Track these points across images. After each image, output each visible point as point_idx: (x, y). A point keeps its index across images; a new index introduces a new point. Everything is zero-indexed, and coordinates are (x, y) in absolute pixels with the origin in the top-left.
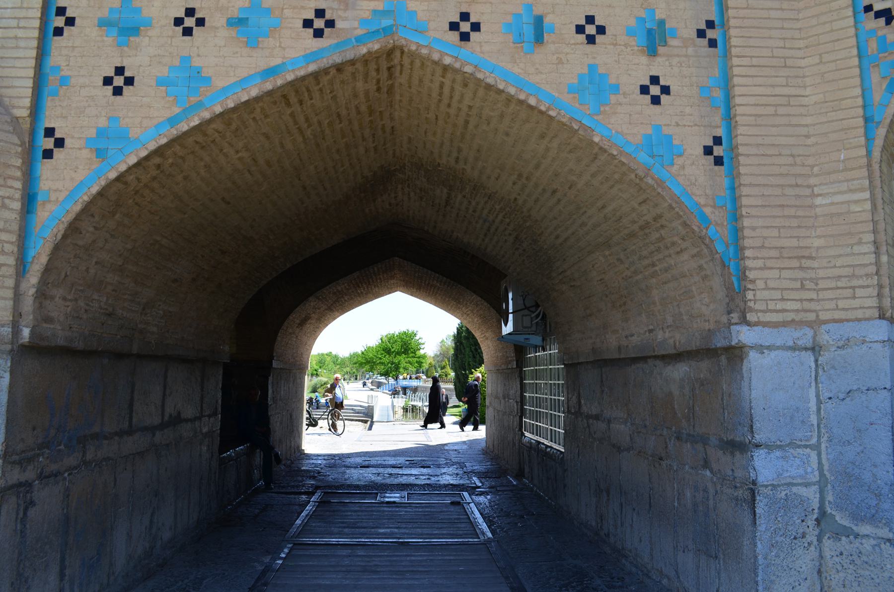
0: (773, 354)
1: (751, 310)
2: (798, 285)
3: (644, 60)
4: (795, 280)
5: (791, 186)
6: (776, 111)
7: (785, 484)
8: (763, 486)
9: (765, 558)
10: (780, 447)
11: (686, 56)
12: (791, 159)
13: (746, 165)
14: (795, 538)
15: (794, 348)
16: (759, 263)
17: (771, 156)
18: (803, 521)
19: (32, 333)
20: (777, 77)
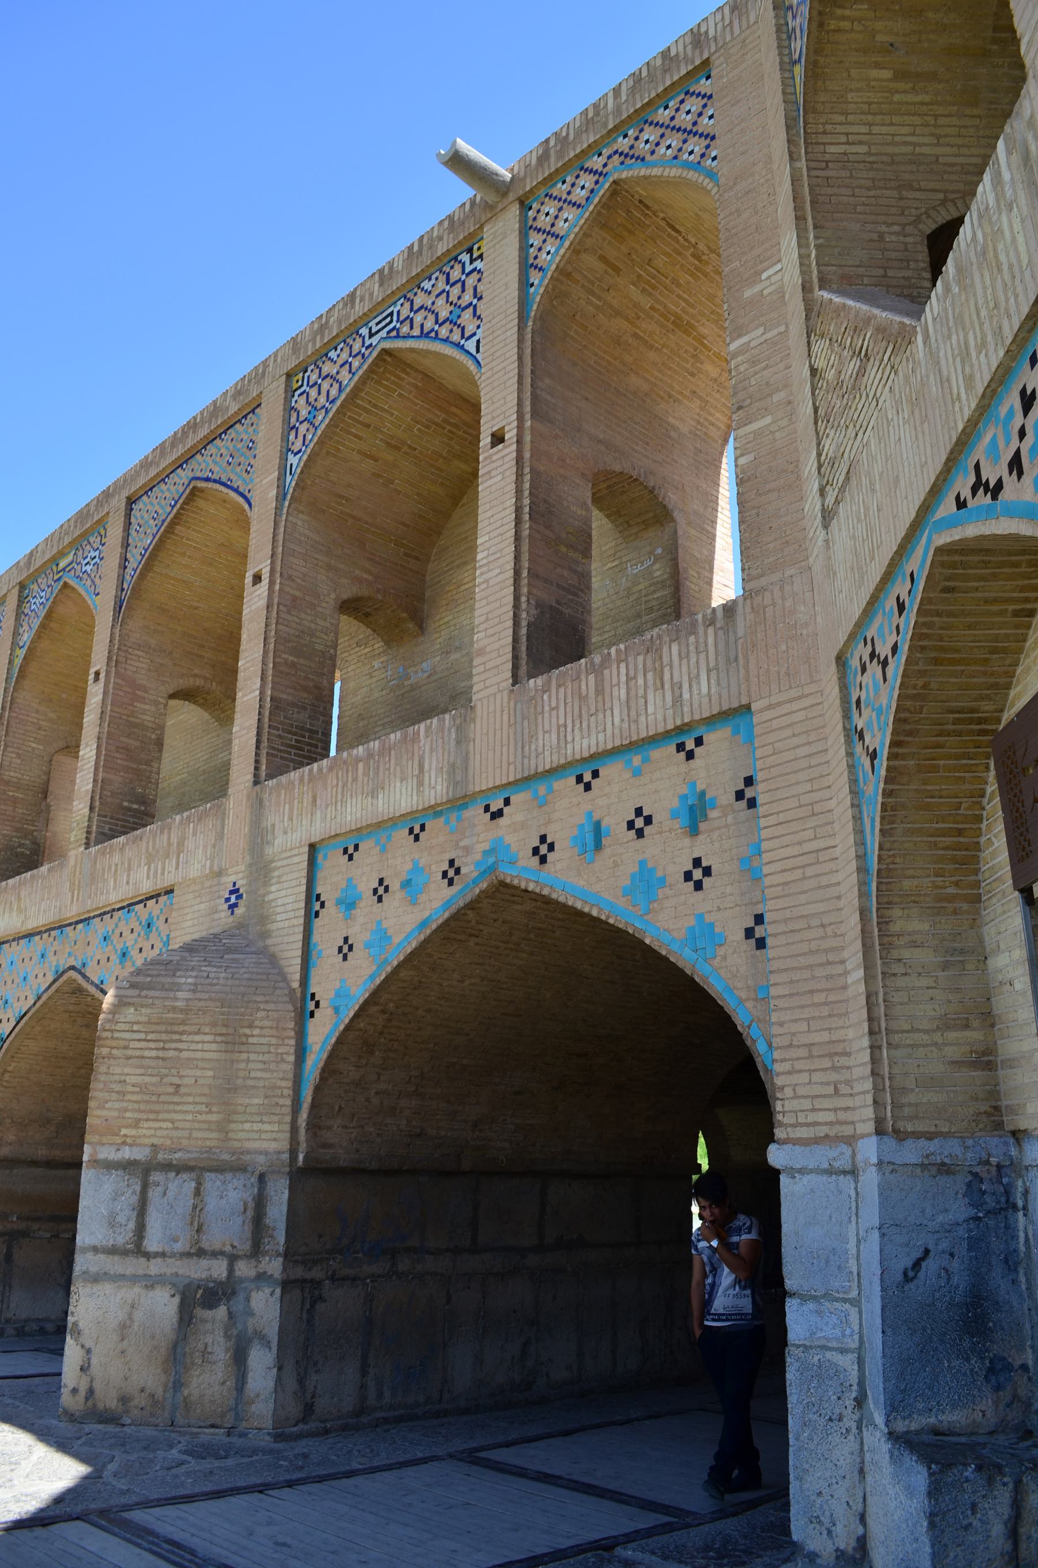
0: (806, 1179)
1: (781, 1124)
2: (831, 1090)
3: (687, 841)
4: (828, 1084)
5: (821, 965)
6: (803, 874)
7: (819, 1347)
8: (793, 1345)
9: (797, 1439)
10: (814, 1298)
12: (821, 930)
13: (773, 948)
14: (830, 1420)
15: (830, 1172)
16: (786, 1066)
17: (799, 931)
18: (839, 1398)
19: (306, 1158)
20: (804, 830)
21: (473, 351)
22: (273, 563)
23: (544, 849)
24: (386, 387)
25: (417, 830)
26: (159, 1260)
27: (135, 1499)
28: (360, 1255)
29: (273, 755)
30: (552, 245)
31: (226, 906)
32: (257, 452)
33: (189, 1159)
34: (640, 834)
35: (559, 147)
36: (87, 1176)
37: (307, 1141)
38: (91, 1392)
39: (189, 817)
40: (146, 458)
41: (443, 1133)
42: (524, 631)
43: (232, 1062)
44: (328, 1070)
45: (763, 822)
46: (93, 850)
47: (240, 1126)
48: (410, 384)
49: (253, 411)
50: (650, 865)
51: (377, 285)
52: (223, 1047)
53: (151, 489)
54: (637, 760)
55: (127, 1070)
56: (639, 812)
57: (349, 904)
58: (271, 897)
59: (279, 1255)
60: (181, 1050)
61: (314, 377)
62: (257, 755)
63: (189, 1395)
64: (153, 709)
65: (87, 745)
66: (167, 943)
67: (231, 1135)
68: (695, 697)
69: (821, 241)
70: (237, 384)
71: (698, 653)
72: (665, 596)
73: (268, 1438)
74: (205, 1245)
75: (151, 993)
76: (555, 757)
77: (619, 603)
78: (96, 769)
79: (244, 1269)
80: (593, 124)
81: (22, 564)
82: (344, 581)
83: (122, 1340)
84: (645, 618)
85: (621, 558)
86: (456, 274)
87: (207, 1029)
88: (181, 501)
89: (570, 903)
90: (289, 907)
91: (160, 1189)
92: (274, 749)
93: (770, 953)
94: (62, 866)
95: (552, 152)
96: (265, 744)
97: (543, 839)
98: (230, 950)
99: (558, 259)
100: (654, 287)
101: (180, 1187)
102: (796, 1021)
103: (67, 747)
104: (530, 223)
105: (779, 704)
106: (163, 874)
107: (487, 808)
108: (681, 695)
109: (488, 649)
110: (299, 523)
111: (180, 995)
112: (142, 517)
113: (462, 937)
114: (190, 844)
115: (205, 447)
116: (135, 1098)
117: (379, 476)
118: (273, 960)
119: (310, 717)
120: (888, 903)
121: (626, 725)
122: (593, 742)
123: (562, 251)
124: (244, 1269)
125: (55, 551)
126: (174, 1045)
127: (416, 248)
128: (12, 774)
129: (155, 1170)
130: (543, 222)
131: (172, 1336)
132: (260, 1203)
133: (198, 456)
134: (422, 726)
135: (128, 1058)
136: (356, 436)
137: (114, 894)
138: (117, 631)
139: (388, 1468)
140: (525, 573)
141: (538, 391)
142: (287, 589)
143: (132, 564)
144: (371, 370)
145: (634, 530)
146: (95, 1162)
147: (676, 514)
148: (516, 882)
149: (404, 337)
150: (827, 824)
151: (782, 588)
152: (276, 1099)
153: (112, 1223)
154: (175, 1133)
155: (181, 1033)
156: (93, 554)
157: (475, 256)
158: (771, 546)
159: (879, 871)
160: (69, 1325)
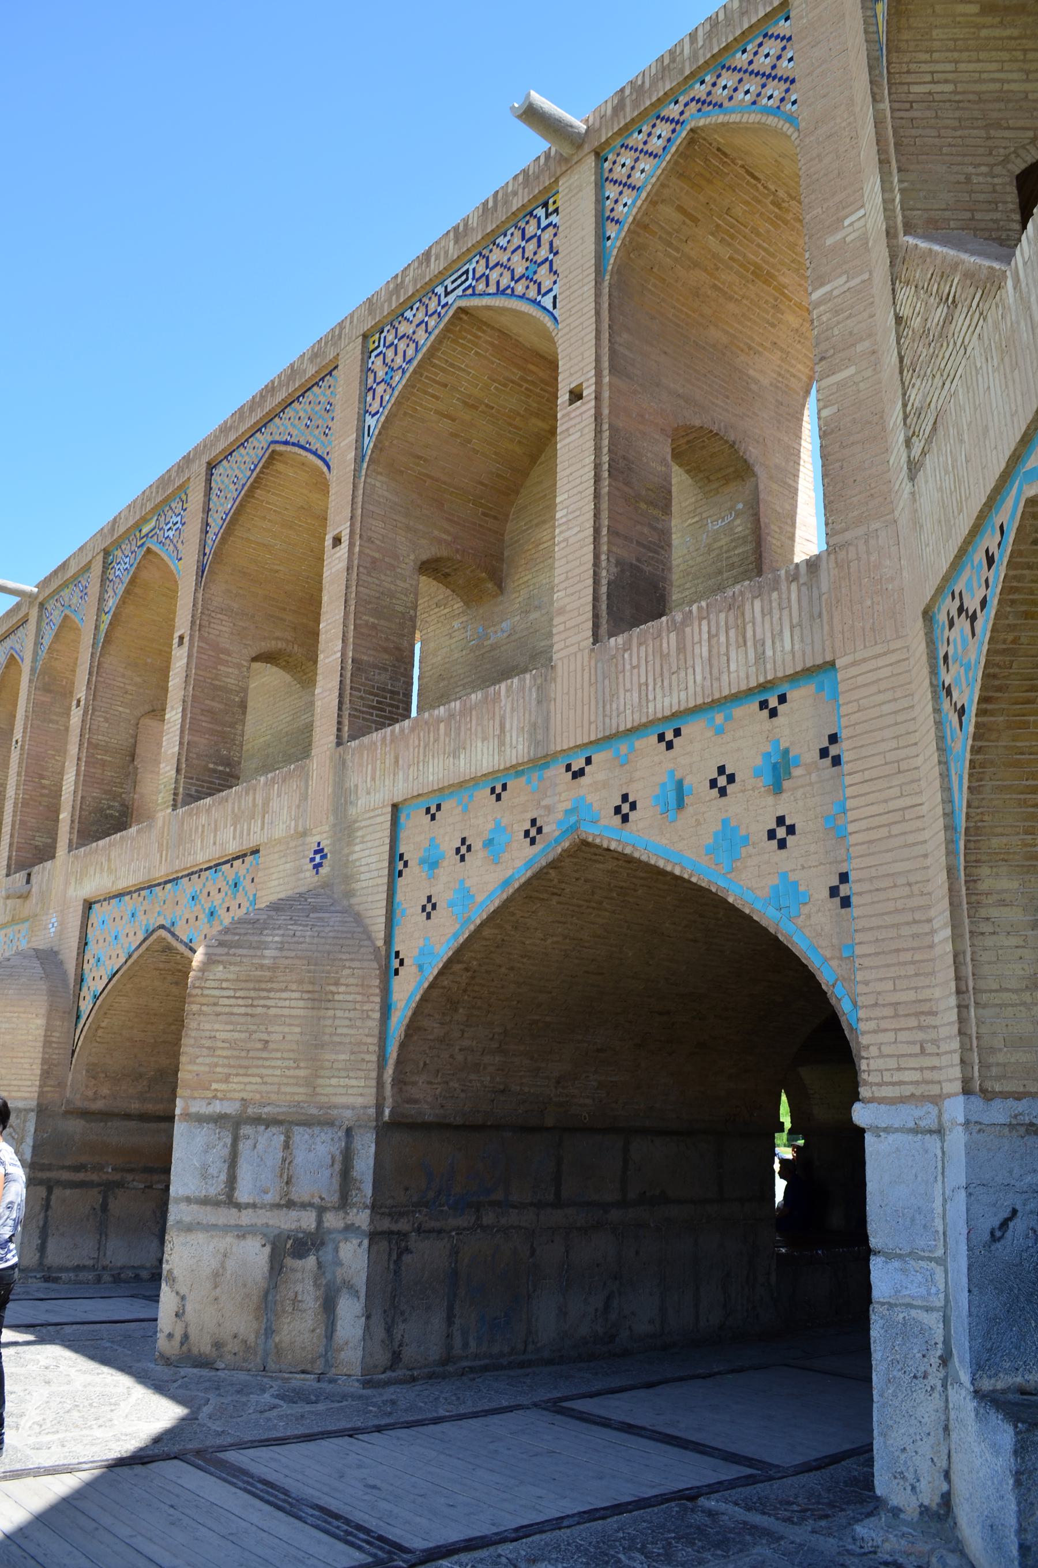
0: (891, 1138)
1: (866, 1083)
2: (917, 1049)
3: (770, 800)
4: (914, 1043)
5: (907, 923)
6: (889, 832)
7: (904, 1305)
8: (878, 1303)
9: (881, 1396)
10: (900, 1257)
11: (811, 784)
12: (907, 888)
13: (859, 906)
14: (915, 1377)
15: (916, 1131)
16: (871, 1025)
17: (885, 889)
18: (924, 1356)
19: (392, 1113)
20: (890, 787)
21: (550, 307)
22: (352, 525)
23: (626, 808)
24: (462, 345)
25: (498, 790)
26: (250, 1210)
27: (229, 1440)
28: (445, 1208)
29: (355, 716)
30: (629, 197)
31: (311, 866)
32: (335, 414)
33: (278, 1113)
34: (723, 792)
35: (634, 97)
36: (180, 1128)
37: (393, 1096)
38: (186, 1337)
39: (273, 778)
40: (226, 422)
41: (526, 1089)
42: (604, 589)
43: (319, 1019)
44: (413, 1028)
45: (848, 780)
46: (180, 811)
47: (327, 1081)
48: (486, 342)
49: (330, 373)
50: (733, 823)
51: (452, 243)
52: (310, 1004)
53: (231, 454)
54: (719, 718)
55: (217, 1026)
56: (721, 770)
57: (432, 864)
58: (355, 856)
59: (366, 1207)
60: (269, 1007)
61: (390, 338)
62: (339, 716)
63: (281, 1342)
64: (236, 672)
65: (172, 709)
66: (254, 902)
67: (318, 1090)
68: (779, 653)
69: (906, 184)
70: (313, 347)
71: (781, 609)
72: (747, 552)
73: (357, 1384)
74: (294, 1197)
75: (240, 951)
76: (636, 716)
77: (699, 559)
78: (182, 732)
79: (333, 1221)
80: (670, 71)
81: (105, 530)
82: (423, 542)
83: (216, 1287)
84: (725, 575)
85: (701, 514)
86: (531, 229)
87: (294, 987)
88: (260, 465)
89: (652, 862)
90: (373, 867)
91: (249, 1143)
92: (356, 710)
93: (855, 911)
94: (150, 826)
95: (628, 102)
96: (347, 705)
97: (625, 798)
98: (315, 909)
99: (635, 210)
100: (732, 237)
101: (270, 1141)
102: (881, 980)
103: (153, 711)
104: (606, 175)
105: (864, 660)
106: (248, 834)
107: (568, 768)
108: (764, 653)
109: (568, 608)
110: (378, 484)
111: (267, 953)
112: (223, 482)
113: (545, 896)
114: (274, 804)
115: (283, 411)
116: (225, 1053)
117: (456, 436)
118: (358, 918)
119: (391, 678)
120: (976, 861)
121: (708, 683)
122: (675, 701)
123: (639, 203)
124: (333, 1221)
125: (138, 517)
126: (262, 1002)
127: (491, 204)
128: (100, 737)
129: (245, 1124)
130: (619, 173)
131: (264, 1285)
132: (347, 1157)
133: (277, 420)
134: (503, 686)
135: (218, 1015)
136: (433, 396)
137: (202, 854)
138: (200, 596)
139: (475, 1415)
140: (604, 531)
141: (616, 346)
142: (367, 551)
143: (214, 528)
144: (447, 329)
145: (715, 485)
146: (187, 1116)
147: (757, 469)
148: (598, 841)
149: (480, 295)
150: (913, 781)
151: (866, 542)
152: (363, 1056)
153: (205, 1176)
154: (264, 1088)
155: (269, 991)
156: (175, 519)
157: (550, 210)
158: (855, 499)
159: (967, 829)
160: (164, 1273)
